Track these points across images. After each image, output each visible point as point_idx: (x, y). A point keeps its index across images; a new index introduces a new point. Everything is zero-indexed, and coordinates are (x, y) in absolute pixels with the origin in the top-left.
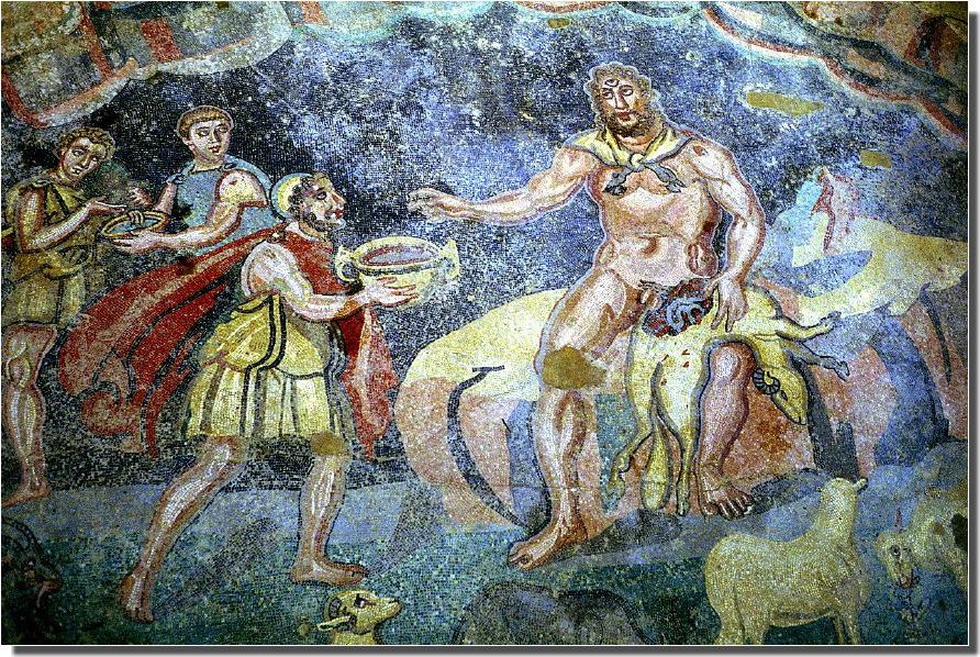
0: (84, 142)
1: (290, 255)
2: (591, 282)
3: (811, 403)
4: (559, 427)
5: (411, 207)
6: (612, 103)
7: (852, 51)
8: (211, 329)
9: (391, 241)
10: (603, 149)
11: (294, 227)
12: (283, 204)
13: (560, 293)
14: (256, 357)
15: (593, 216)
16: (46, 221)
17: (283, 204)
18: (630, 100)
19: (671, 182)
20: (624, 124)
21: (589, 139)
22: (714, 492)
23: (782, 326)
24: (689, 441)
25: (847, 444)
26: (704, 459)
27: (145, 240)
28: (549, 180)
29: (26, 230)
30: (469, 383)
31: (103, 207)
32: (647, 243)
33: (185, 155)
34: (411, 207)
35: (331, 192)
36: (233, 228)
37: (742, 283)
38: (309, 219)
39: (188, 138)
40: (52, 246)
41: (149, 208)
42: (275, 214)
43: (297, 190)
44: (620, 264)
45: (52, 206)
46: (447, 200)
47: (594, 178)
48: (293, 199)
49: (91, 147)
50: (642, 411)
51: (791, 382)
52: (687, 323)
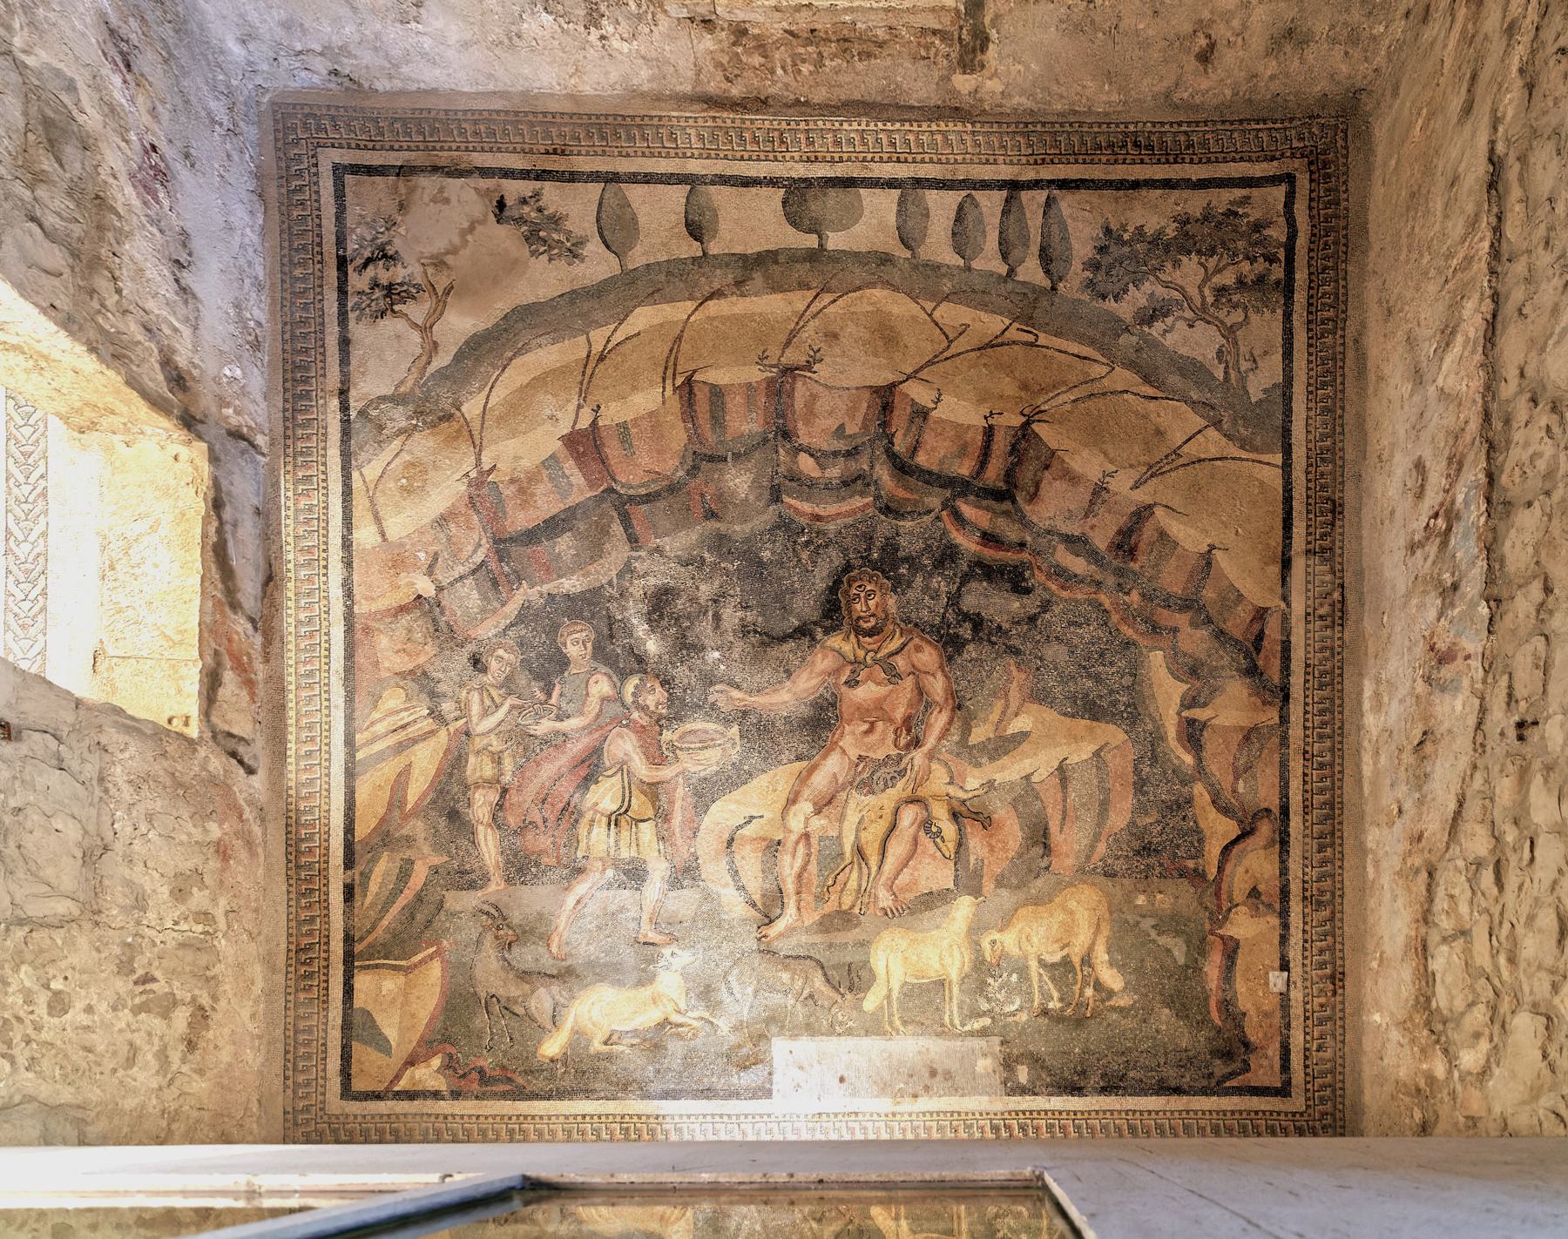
0: (501, 652)
1: (633, 736)
2: (825, 757)
3: (960, 845)
4: (794, 856)
5: (711, 699)
6: (858, 607)
7: (1061, 547)
8: (588, 789)
9: (699, 725)
10: (847, 648)
11: (636, 715)
12: (629, 699)
13: (805, 763)
14: (615, 807)
15: (834, 705)
16: (485, 713)
17: (629, 699)
18: (871, 603)
19: (894, 675)
20: (865, 626)
21: (835, 641)
22: (885, 900)
23: (952, 790)
24: (874, 869)
25: (977, 875)
26: (883, 879)
27: (545, 726)
28: (805, 675)
29: (475, 719)
30: (741, 827)
31: (518, 702)
32: (866, 727)
33: (563, 662)
34: (711, 699)
35: (659, 689)
36: (598, 716)
37: (931, 756)
38: (644, 708)
39: (565, 644)
40: (490, 731)
41: (546, 702)
42: (623, 705)
43: (636, 687)
44: (847, 742)
45: (488, 702)
46: (736, 694)
47: (837, 672)
48: (634, 694)
49: (506, 656)
50: (848, 849)
51: (949, 829)
52: (886, 786)
